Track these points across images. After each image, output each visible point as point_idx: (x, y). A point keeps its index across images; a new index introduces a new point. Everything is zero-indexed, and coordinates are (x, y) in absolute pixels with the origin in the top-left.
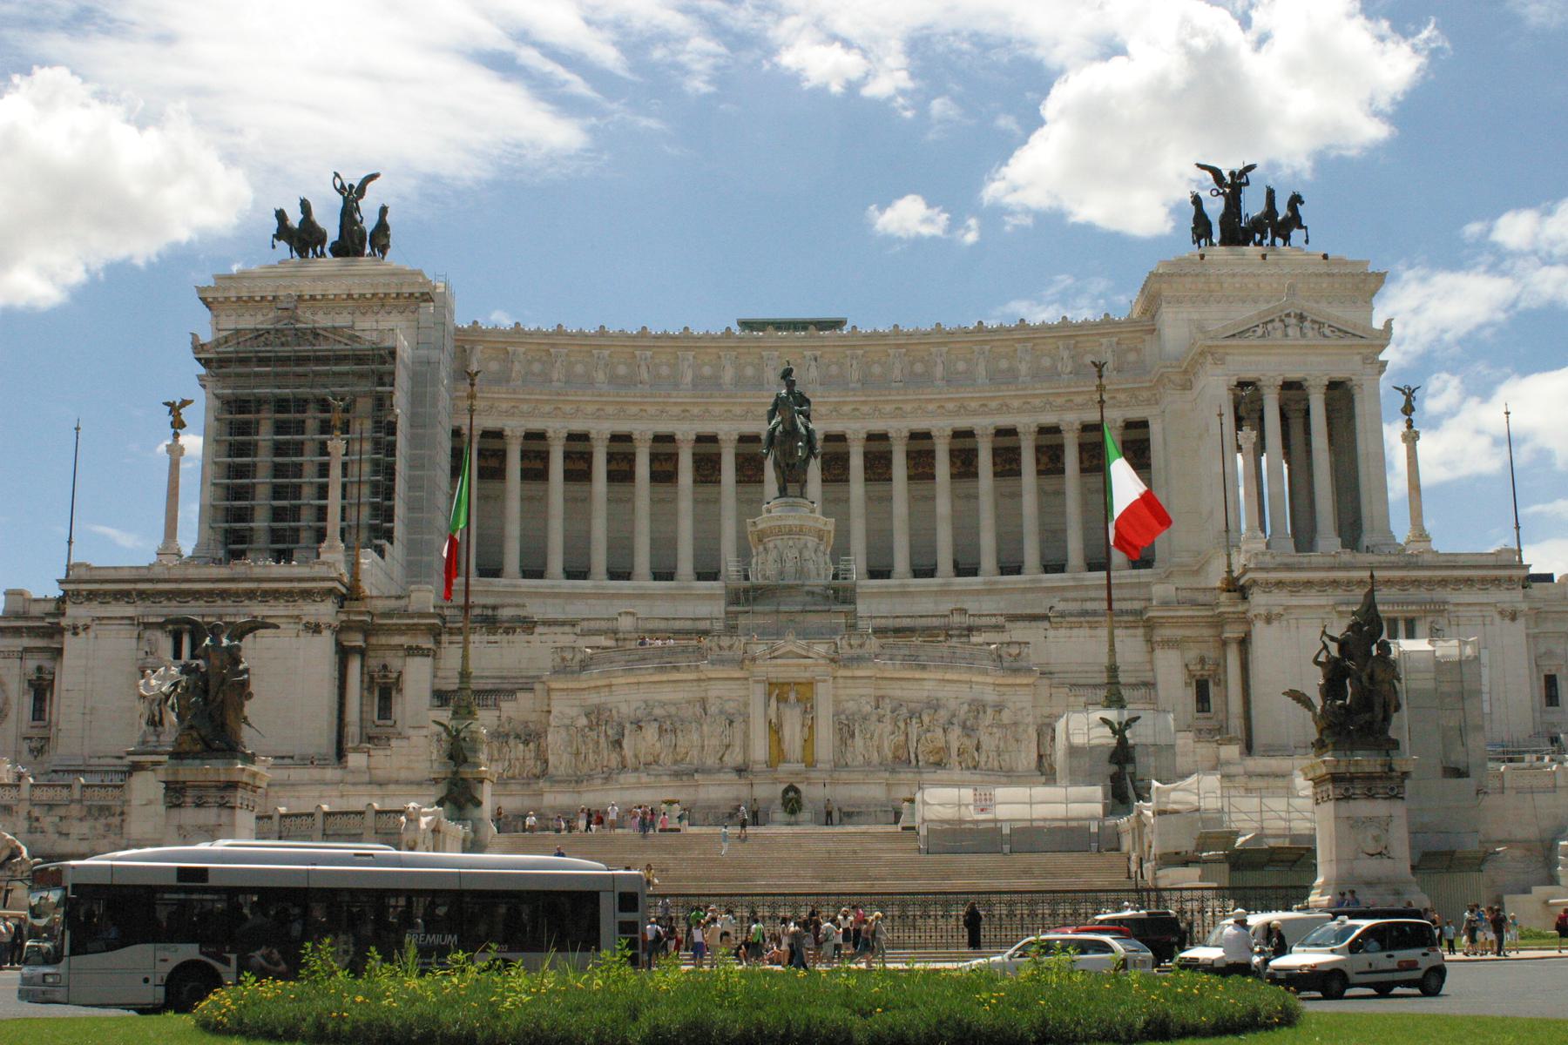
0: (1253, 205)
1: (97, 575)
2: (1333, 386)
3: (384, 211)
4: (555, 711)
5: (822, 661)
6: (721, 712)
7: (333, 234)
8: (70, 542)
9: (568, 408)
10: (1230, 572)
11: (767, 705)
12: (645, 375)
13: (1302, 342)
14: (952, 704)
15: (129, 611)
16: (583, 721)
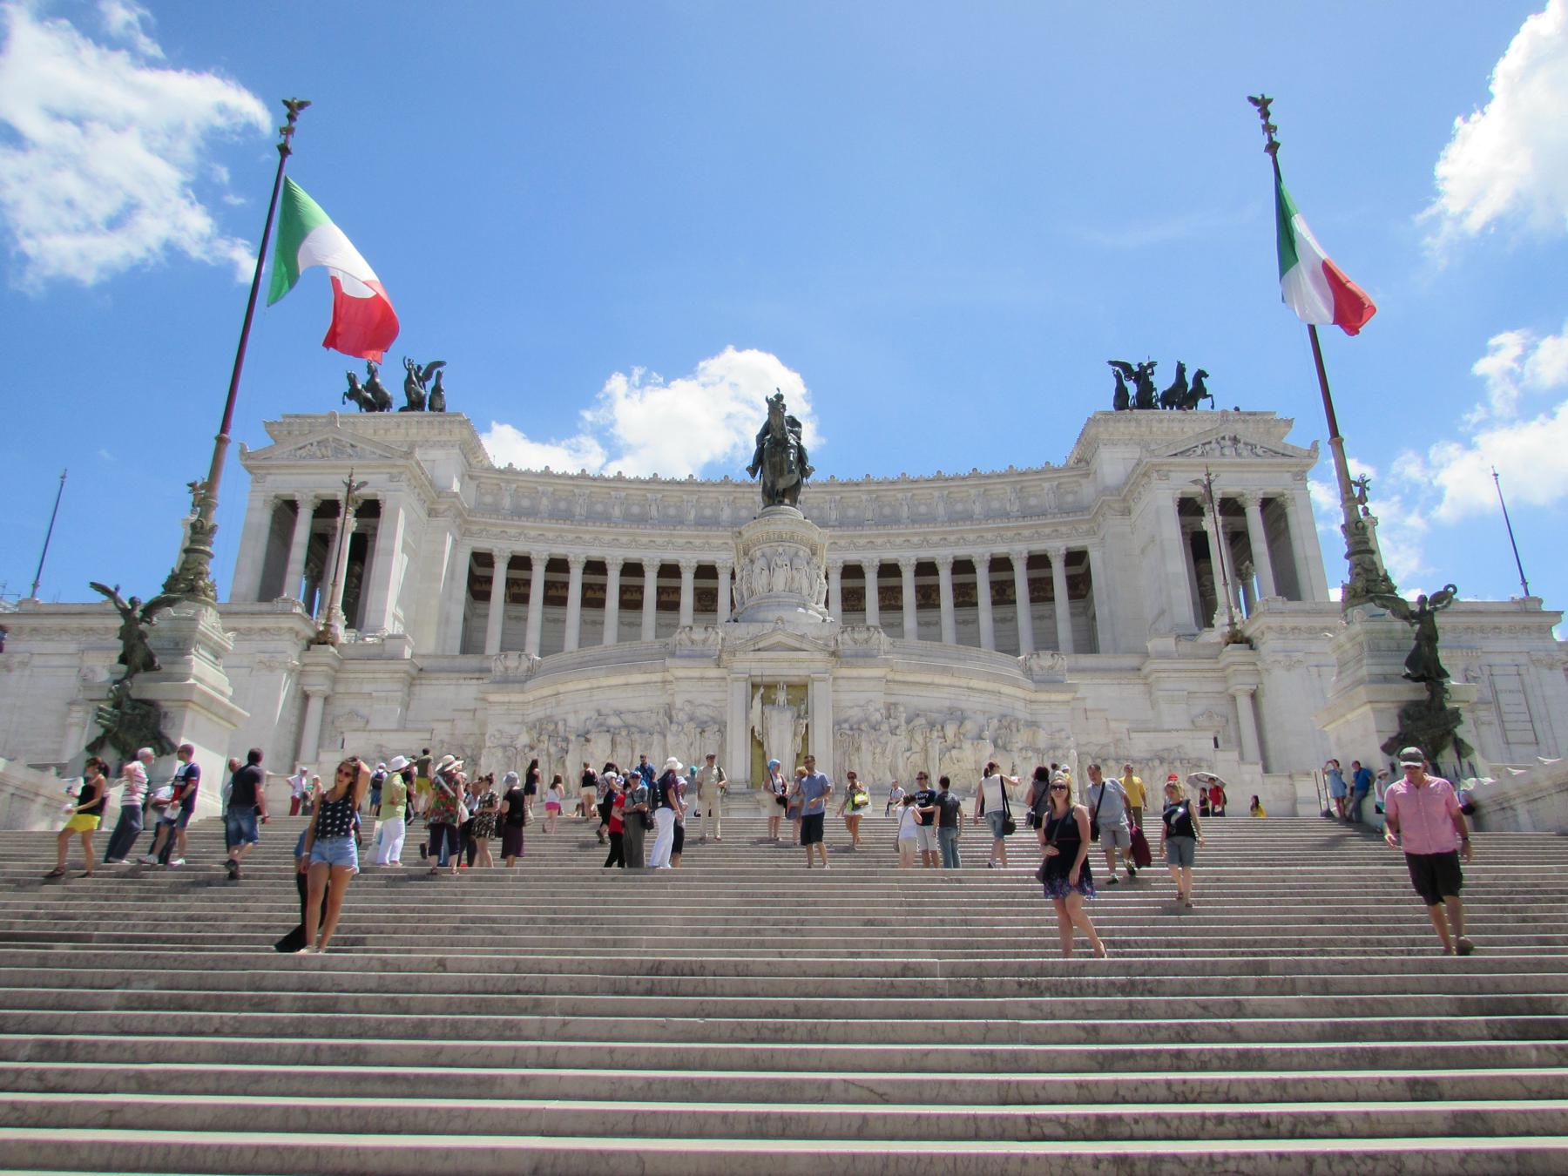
0: (1162, 381)
1: (44, 610)
2: (1267, 504)
3: (439, 375)
4: (491, 730)
5: (819, 656)
6: (691, 719)
7: (399, 398)
8: (36, 585)
9: (587, 537)
10: (1232, 624)
11: (749, 707)
12: (654, 512)
13: (1238, 460)
14: (981, 719)
15: (72, 647)
16: (524, 739)
